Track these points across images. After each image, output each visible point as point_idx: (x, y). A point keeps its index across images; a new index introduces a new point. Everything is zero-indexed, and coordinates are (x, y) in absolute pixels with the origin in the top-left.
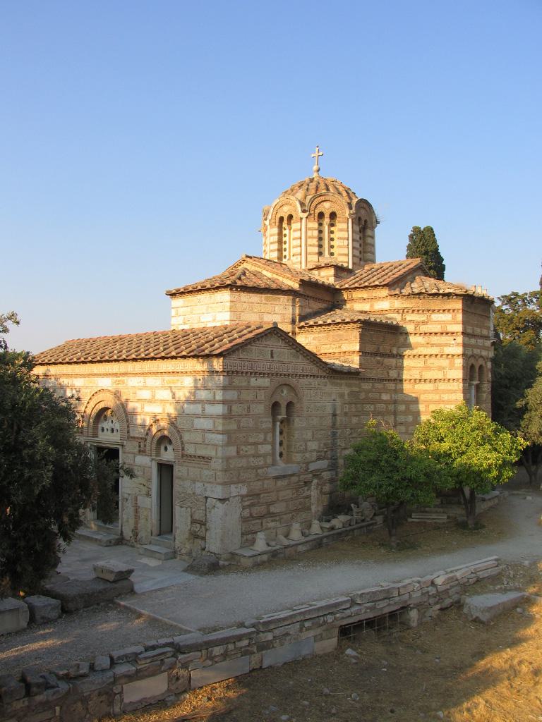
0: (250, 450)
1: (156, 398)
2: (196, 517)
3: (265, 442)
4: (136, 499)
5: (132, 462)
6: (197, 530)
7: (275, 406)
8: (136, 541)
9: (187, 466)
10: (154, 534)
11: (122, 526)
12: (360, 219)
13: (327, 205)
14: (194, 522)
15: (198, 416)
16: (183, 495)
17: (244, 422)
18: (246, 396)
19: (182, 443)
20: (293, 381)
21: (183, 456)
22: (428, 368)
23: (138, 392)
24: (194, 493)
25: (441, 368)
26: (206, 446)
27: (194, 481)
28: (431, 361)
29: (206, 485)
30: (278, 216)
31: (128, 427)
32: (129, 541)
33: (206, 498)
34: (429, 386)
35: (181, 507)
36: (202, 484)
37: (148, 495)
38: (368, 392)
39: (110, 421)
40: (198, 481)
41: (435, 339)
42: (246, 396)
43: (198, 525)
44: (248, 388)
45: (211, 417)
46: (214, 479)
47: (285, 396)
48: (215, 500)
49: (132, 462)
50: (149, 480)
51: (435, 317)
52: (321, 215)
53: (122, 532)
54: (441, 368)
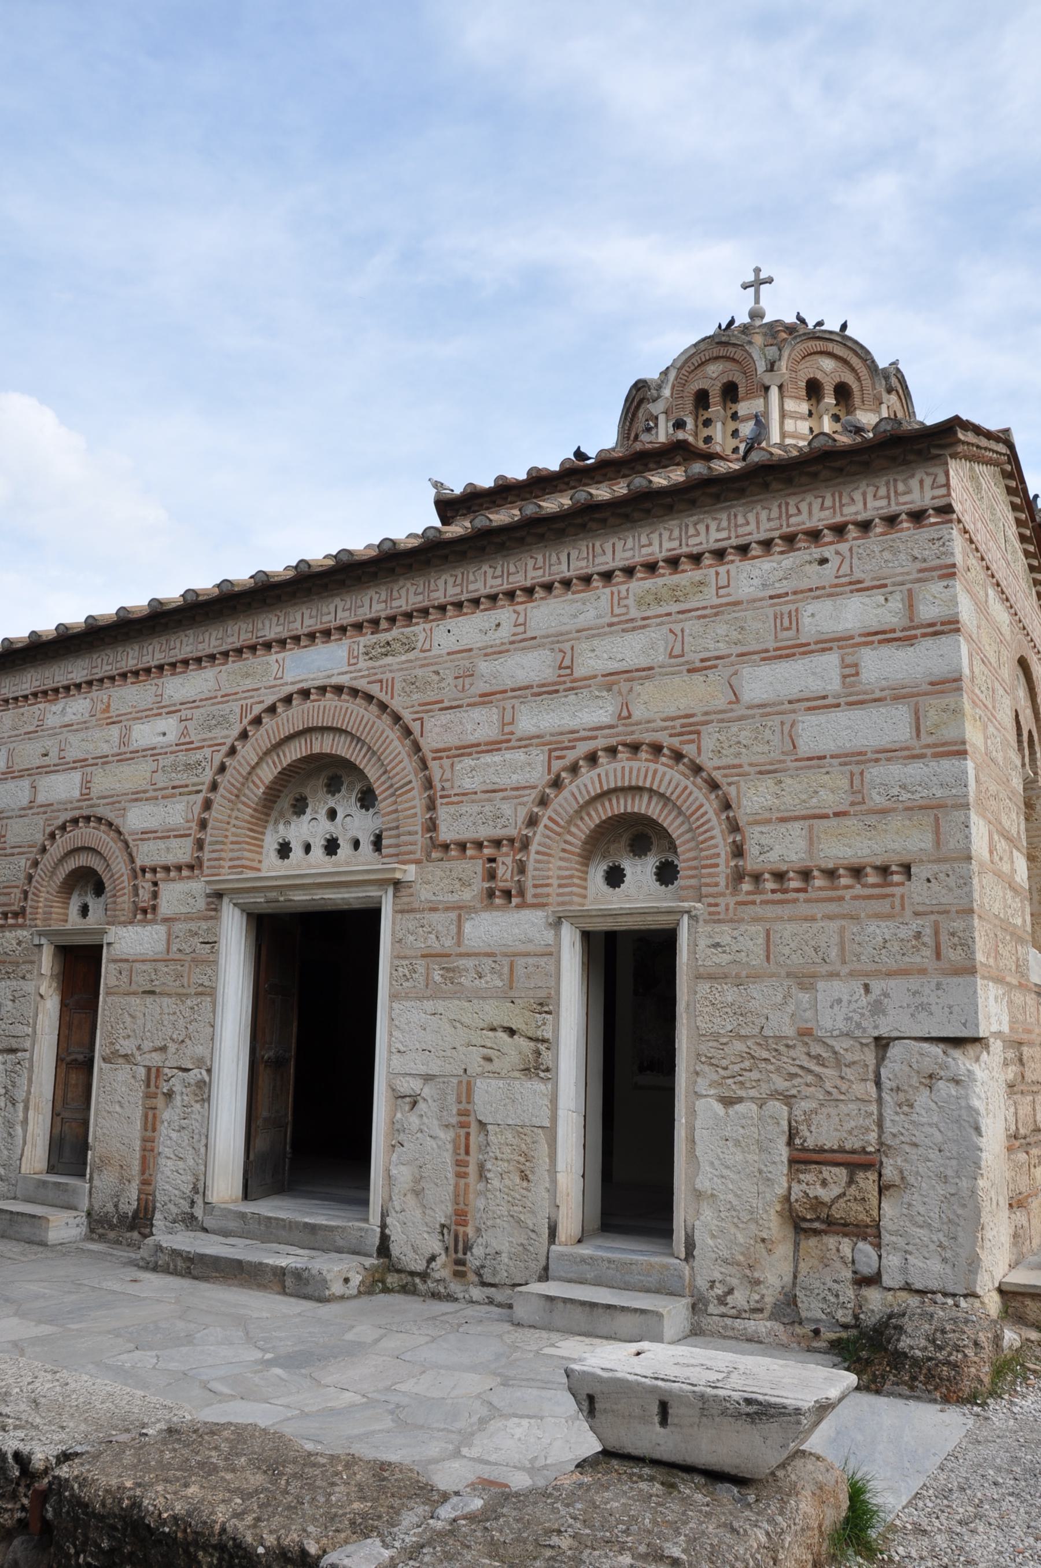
1: (580, 672)
2: (823, 1133)
4: (467, 1092)
5: (448, 942)
6: (825, 1195)
8: (459, 1275)
9: (756, 920)
10: (562, 1234)
11: (384, 1215)
14: (803, 1158)
15: (819, 703)
16: (739, 1046)
19: (734, 827)
21: (739, 876)
23: (484, 667)
24: (805, 1033)
26: (872, 820)
27: (805, 980)
29: (877, 986)
30: (696, 386)
31: (431, 806)
32: (424, 1276)
33: (882, 1044)
35: (728, 1102)
36: (858, 987)
37: (538, 1068)
39: (323, 812)
40: (833, 975)
43: (842, 1173)
45: (898, 694)
46: (928, 952)
48: (937, 1050)
49: (448, 942)
50: (546, 1006)
53: (385, 1239)
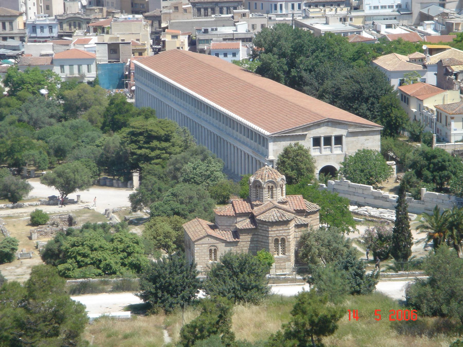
0: (203, 259)
3: (207, 257)
7: (211, 250)
12: (269, 187)
13: (258, 183)
17: (201, 253)
18: (201, 248)
20: (216, 245)
22: (263, 239)
25: (266, 239)
28: (264, 237)
34: (263, 244)
38: (243, 245)
41: (264, 232)
42: (201, 248)
44: (202, 247)
47: (213, 248)
51: (264, 226)
52: (256, 186)
54: (266, 239)
